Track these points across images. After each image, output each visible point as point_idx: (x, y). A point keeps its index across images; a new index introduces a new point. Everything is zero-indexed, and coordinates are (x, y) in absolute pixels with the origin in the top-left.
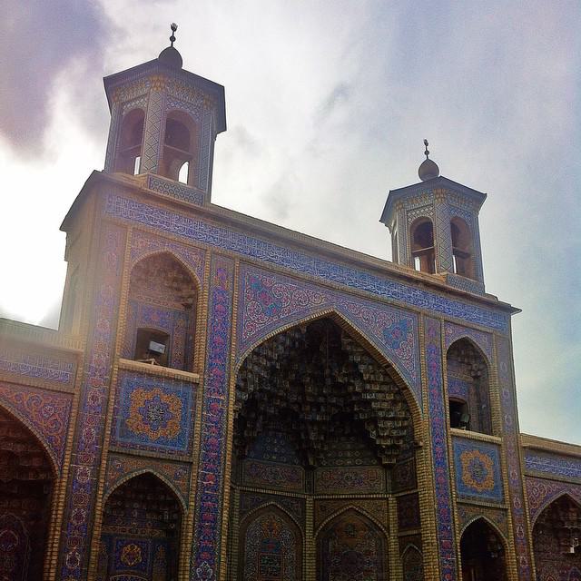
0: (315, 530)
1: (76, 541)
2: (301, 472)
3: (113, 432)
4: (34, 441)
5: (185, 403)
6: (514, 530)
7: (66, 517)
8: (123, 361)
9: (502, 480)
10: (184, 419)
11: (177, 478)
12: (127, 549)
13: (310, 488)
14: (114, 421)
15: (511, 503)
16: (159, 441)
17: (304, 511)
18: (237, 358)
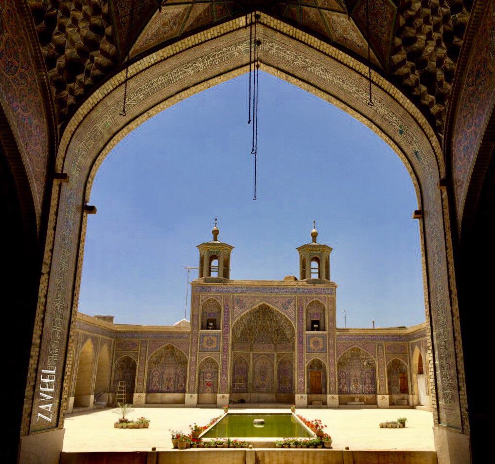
0: (277, 362)
1: (192, 374)
2: (273, 346)
3: (200, 348)
4: (182, 354)
5: (218, 338)
6: (329, 360)
7: (190, 368)
8: (201, 331)
9: (326, 345)
10: (217, 341)
11: (216, 357)
12: (208, 374)
13: (276, 350)
14: (200, 346)
15: (329, 352)
16: (211, 349)
17: (274, 356)
18: (232, 324)
